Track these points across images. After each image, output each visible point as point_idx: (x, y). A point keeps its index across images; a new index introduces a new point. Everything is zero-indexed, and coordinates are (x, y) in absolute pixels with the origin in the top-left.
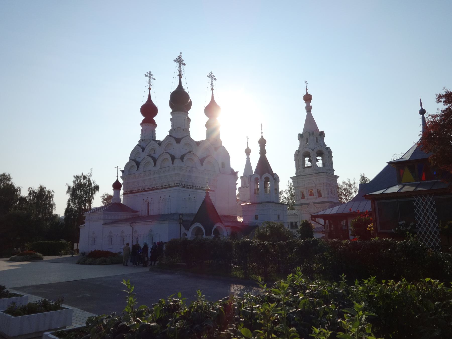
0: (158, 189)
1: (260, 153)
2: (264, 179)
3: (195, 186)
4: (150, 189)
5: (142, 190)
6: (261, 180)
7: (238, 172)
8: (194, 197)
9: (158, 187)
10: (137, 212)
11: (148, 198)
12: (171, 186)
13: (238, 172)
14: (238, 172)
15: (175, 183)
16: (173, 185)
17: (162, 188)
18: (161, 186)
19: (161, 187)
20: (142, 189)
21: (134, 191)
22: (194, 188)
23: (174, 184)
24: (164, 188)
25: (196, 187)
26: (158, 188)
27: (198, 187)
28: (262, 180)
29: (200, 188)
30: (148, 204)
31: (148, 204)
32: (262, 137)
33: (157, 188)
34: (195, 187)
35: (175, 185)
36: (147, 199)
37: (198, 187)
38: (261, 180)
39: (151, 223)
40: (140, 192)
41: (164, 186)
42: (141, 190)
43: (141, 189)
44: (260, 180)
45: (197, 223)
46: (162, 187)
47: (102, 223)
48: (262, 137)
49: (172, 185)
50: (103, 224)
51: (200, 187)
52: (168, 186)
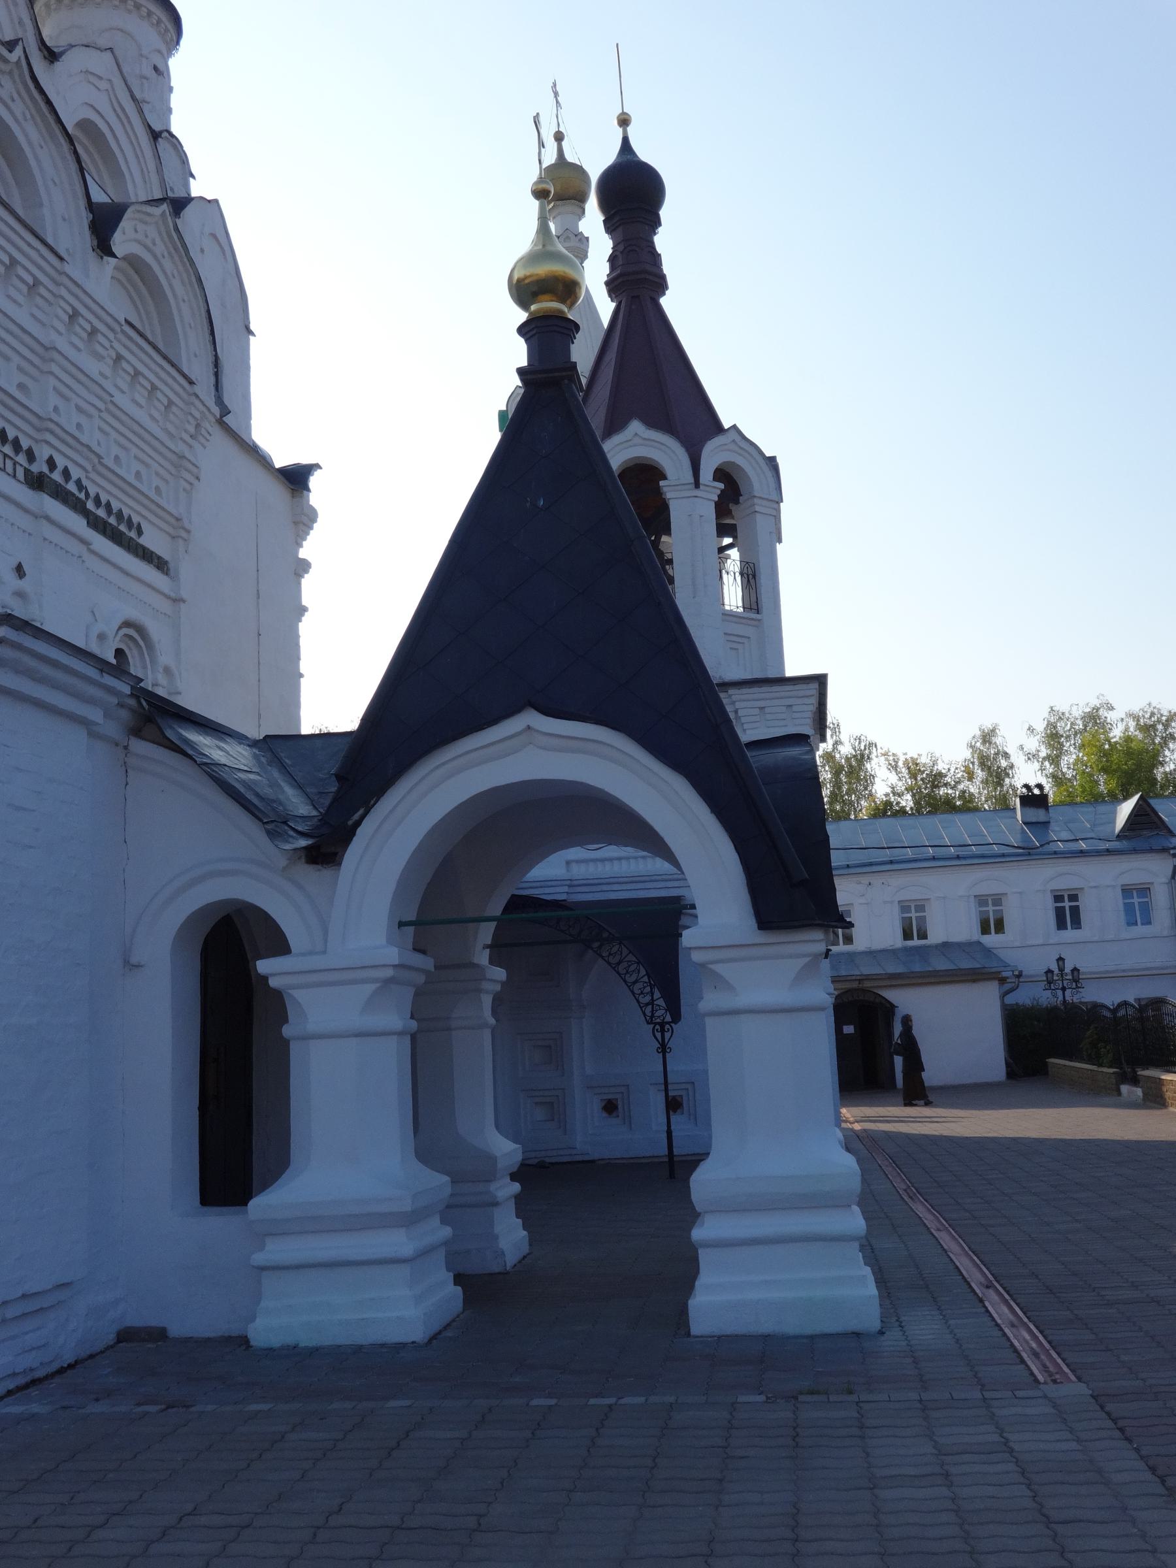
2: (715, 479)
3: (31, 456)
6: (697, 484)
7: (319, 470)
8: (20, 570)
13: (317, 466)
14: (317, 466)
22: (20, 473)
25: (35, 468)
27: (51, 463)
28: (702, 481)
29: (71, 487)
32: (626, 146)
34: (21, 459)
37: (57, 476)
38: (697, 484)
44: (690, 478)
45: (531, 718)
48: (626, 146)
51: (66, 473)
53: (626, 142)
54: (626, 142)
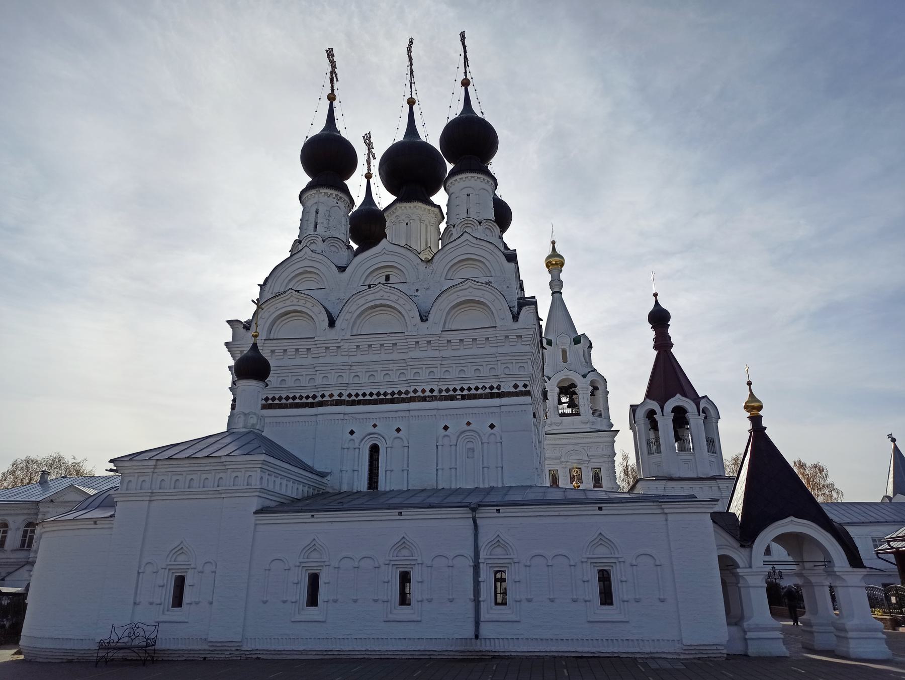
0: (433, 399)
1: (656, 347)
4: (389, 397)
5: (344, 397)
9: (432, 391)
10: (323, 475)
11: (375, 426)
12: (495, 391)
15: (521, 384)
16: (507, 387)
17: (452, 398)
18: (444, 388)
19: (444, 393)
20: (345, 393)
21: (294, 398)
23: (516, 386)
24: (460, 397)
26: (429, 396)
30: (374, 449)
31: (374, 449)
33: (428, 394)
35: (521, 388)
36: (372, 430)
39: (600, 509)
40: (331, 405)
41: (462, 389)
42: (336, 397)
43: (340, 395)
46: (451, 393)
47: (255, 504)
49: (502, 390)
50: (256, 513)
52: (480, 391)
53: (657, 301)
54: (657, 301)
